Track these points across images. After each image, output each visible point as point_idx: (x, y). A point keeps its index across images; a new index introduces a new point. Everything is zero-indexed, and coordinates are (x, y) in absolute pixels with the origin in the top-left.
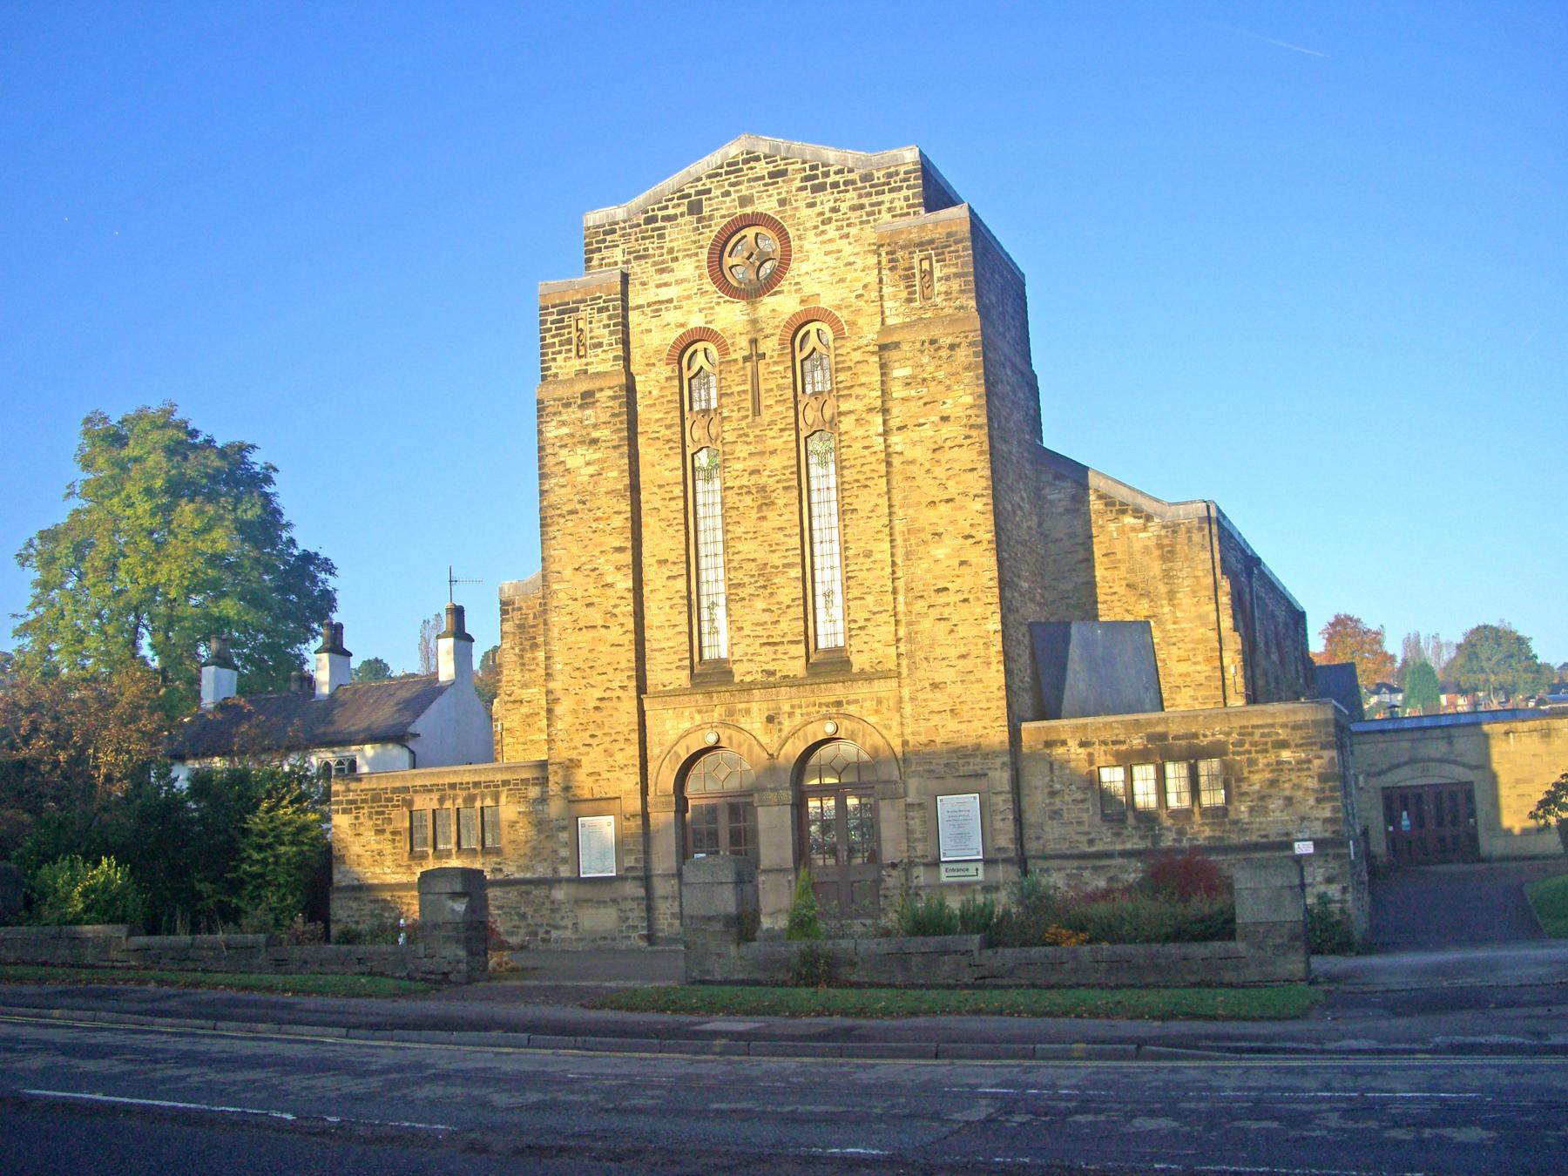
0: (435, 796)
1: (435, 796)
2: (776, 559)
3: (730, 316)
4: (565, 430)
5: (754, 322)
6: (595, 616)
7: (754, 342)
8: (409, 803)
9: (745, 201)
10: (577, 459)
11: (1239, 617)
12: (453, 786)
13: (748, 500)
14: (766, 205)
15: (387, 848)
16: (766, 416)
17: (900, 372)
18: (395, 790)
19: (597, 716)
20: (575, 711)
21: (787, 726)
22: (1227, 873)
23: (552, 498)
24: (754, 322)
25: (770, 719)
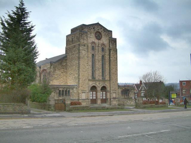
0: (62, 89)
1: (62, 89)
2: (99, 67)
3: (96, 41)
4: (82, 48)
5: (99, 43)
6: (84, 70)
7: (98, 45)
8: (59, 89)
9: (98, 30)
10: (83, 52)
11: (63, 56)
12: (65, 88)
13: (97, 61)
14: (100, 31)
15: (56, 95)
16: (99, 53)
17: (111, 52)
18: (57, 87)
19: (84, 81)
20: (82, 81)
21: (101, 84)
22: (50, 99)
23: (80, 56)
24: (99, 43)
25: (99, 84)
